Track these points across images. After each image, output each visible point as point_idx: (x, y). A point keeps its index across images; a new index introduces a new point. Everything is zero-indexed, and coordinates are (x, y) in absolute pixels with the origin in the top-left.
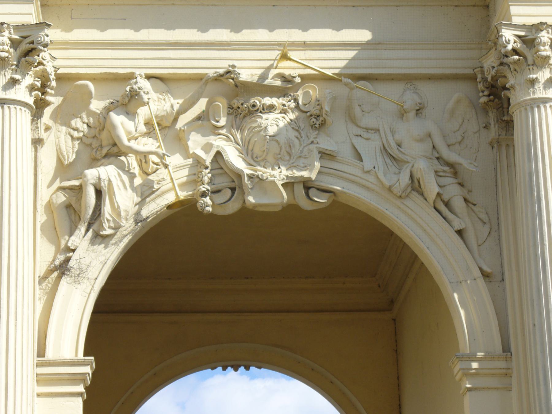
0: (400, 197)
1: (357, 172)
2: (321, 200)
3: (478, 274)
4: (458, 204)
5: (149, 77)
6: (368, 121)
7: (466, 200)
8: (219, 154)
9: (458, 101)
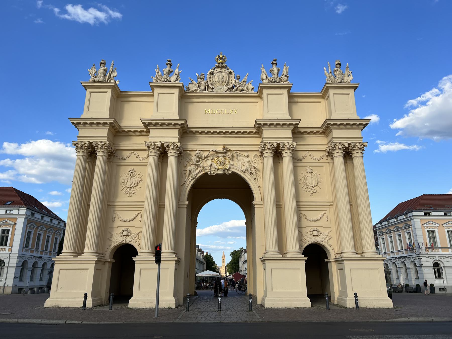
0: (244, 172)
1: (236, 168)
2: (230, 172)
5: (199, 150)
7: (256, 173)
9: (255, 155)
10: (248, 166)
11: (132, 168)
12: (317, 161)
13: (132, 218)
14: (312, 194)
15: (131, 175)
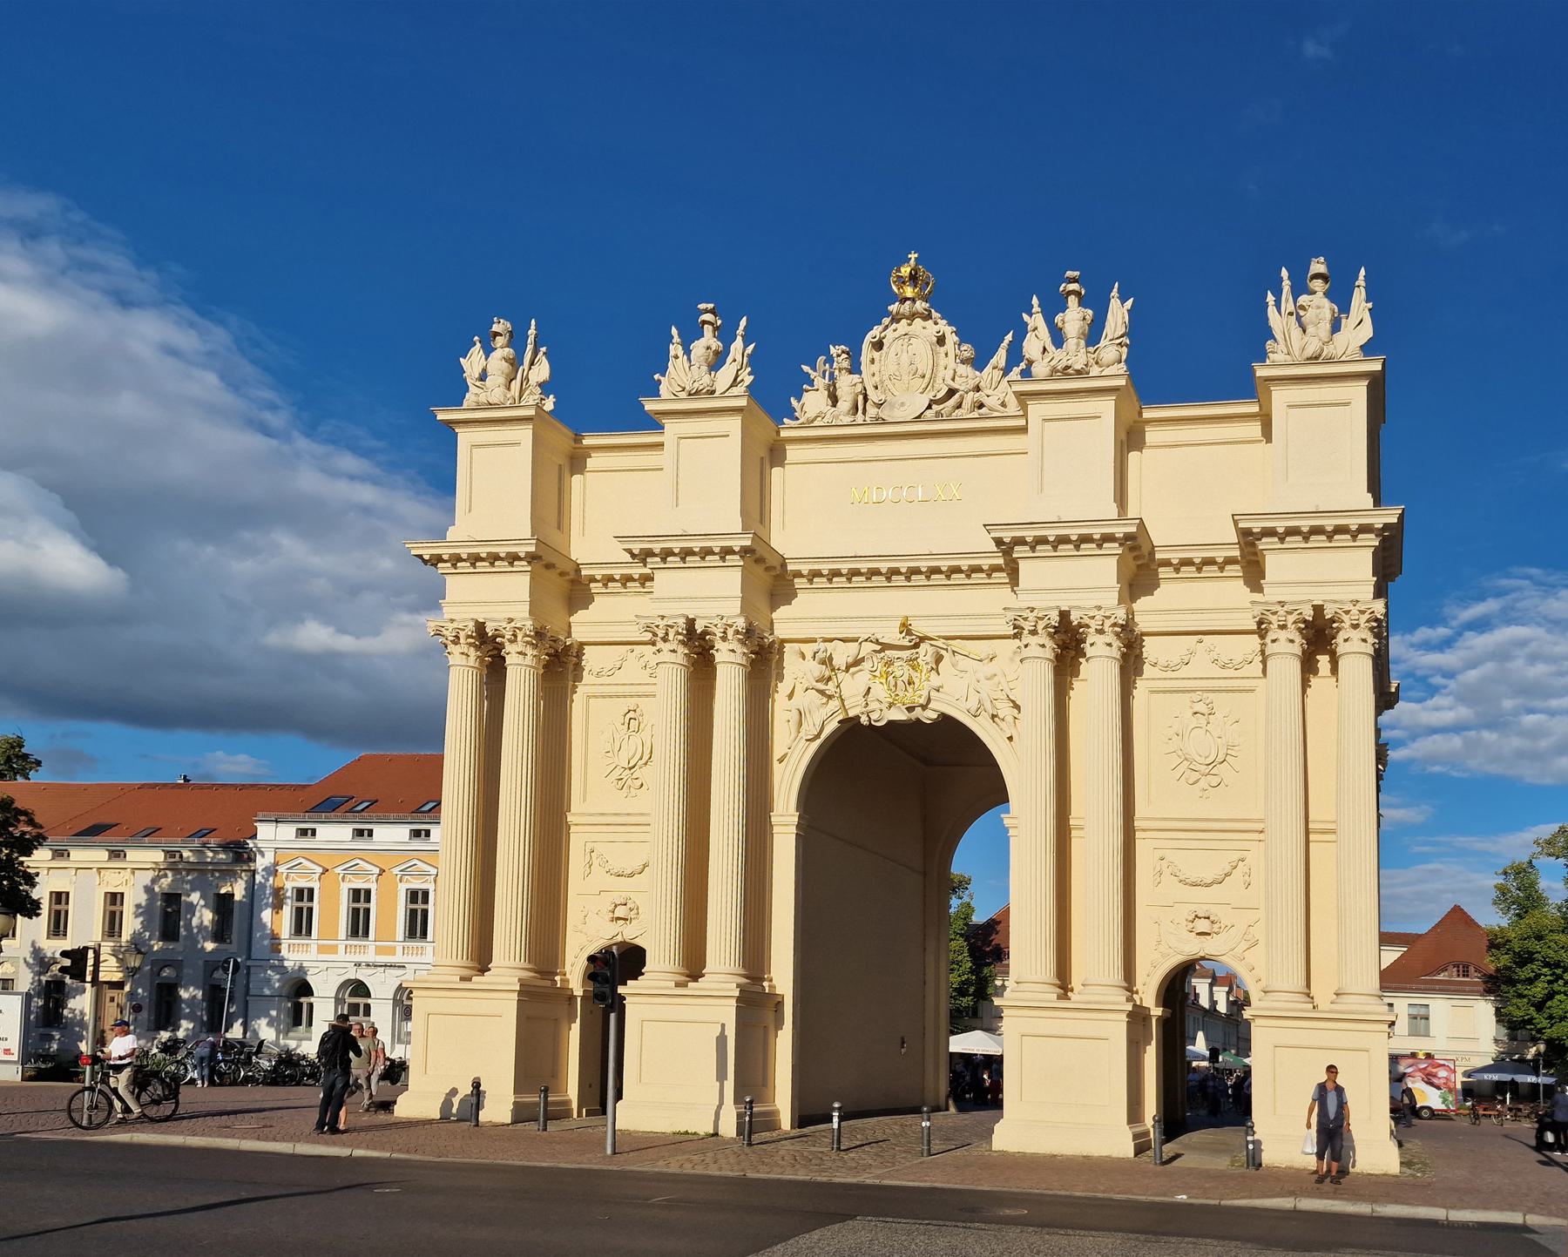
11: (631, 703)
12: (1232, 673)
15: (629, 728)
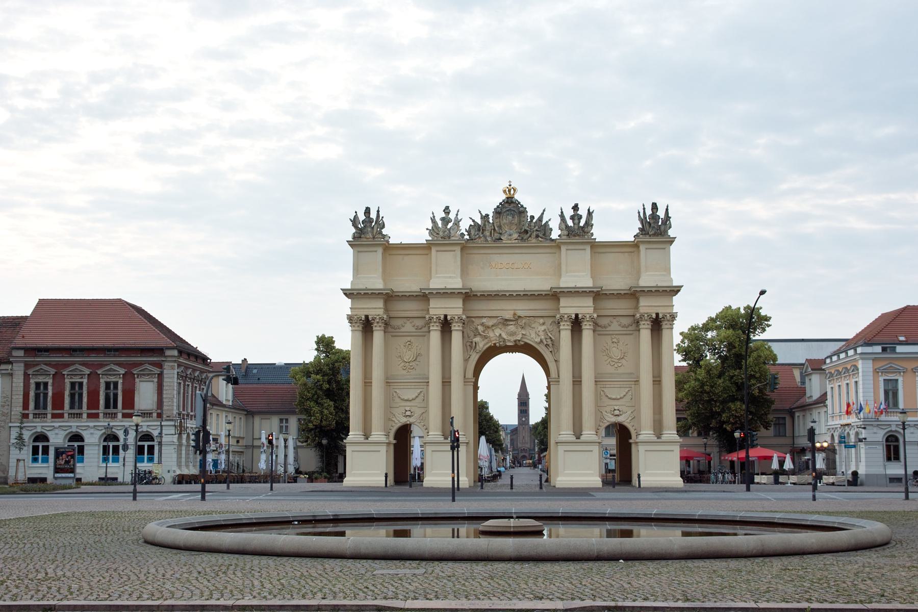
2: (522, 343)
3: (554, 360)
4: (551, 345)
6: (533, 326)
8: (500, 335)
9: (552, 322)
10: (543, 337)
11: (409, 339)
13: (414, 396)
14: (616, 368)
